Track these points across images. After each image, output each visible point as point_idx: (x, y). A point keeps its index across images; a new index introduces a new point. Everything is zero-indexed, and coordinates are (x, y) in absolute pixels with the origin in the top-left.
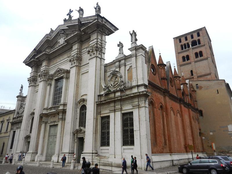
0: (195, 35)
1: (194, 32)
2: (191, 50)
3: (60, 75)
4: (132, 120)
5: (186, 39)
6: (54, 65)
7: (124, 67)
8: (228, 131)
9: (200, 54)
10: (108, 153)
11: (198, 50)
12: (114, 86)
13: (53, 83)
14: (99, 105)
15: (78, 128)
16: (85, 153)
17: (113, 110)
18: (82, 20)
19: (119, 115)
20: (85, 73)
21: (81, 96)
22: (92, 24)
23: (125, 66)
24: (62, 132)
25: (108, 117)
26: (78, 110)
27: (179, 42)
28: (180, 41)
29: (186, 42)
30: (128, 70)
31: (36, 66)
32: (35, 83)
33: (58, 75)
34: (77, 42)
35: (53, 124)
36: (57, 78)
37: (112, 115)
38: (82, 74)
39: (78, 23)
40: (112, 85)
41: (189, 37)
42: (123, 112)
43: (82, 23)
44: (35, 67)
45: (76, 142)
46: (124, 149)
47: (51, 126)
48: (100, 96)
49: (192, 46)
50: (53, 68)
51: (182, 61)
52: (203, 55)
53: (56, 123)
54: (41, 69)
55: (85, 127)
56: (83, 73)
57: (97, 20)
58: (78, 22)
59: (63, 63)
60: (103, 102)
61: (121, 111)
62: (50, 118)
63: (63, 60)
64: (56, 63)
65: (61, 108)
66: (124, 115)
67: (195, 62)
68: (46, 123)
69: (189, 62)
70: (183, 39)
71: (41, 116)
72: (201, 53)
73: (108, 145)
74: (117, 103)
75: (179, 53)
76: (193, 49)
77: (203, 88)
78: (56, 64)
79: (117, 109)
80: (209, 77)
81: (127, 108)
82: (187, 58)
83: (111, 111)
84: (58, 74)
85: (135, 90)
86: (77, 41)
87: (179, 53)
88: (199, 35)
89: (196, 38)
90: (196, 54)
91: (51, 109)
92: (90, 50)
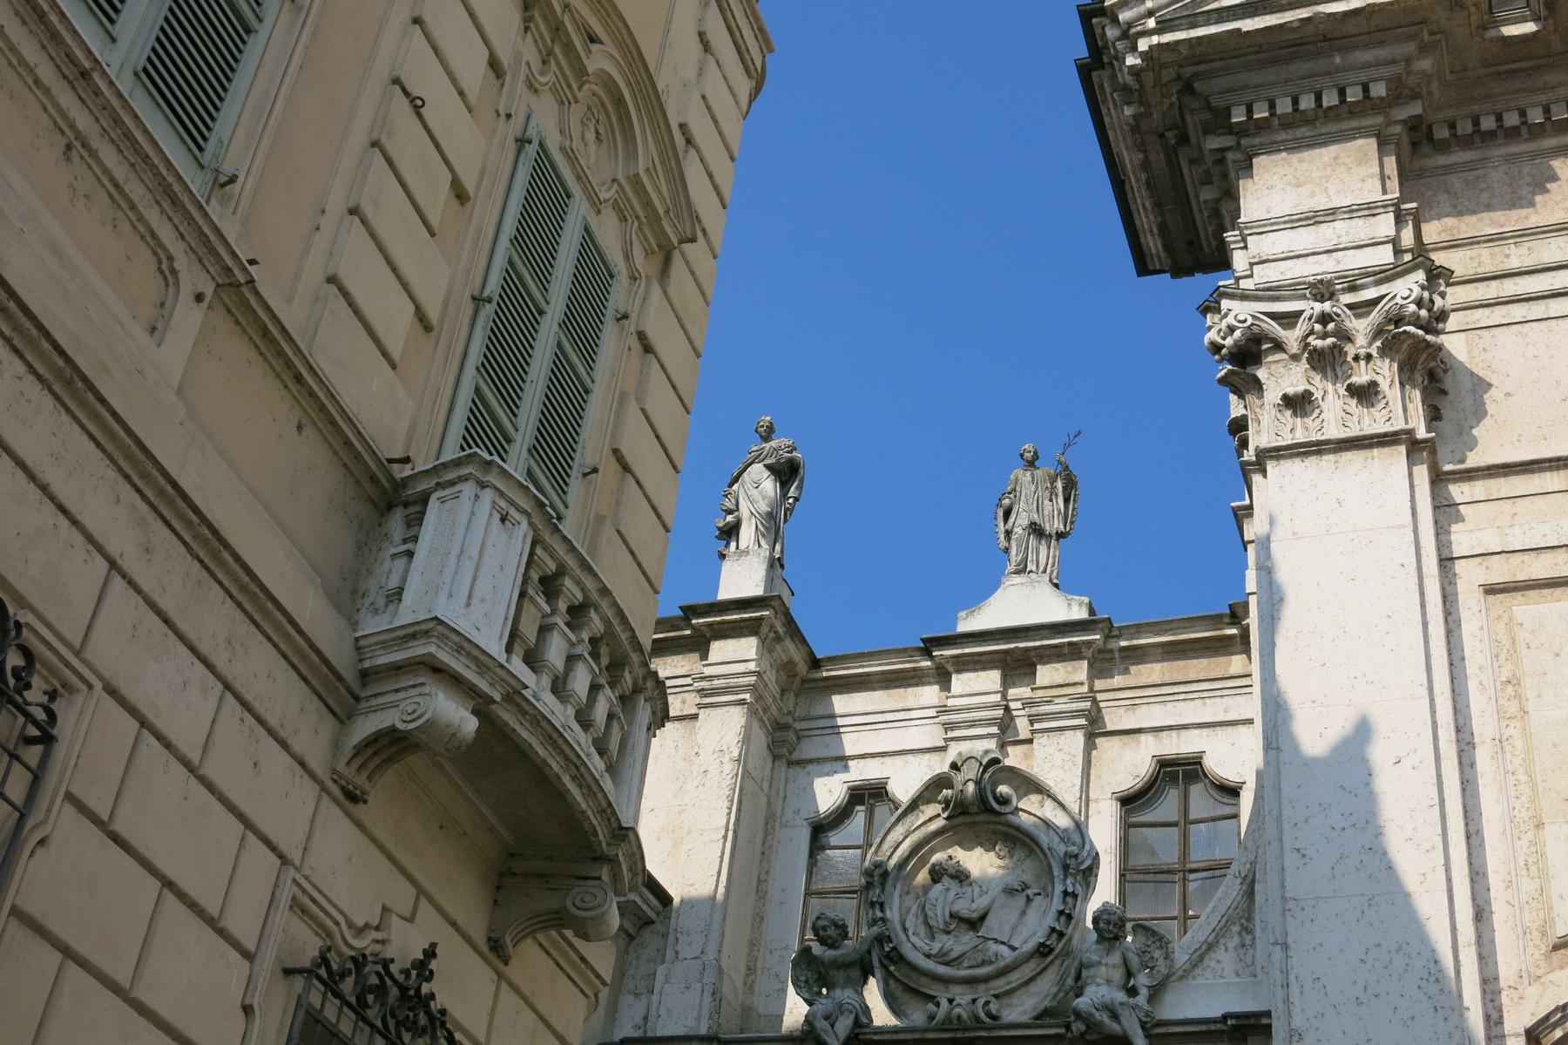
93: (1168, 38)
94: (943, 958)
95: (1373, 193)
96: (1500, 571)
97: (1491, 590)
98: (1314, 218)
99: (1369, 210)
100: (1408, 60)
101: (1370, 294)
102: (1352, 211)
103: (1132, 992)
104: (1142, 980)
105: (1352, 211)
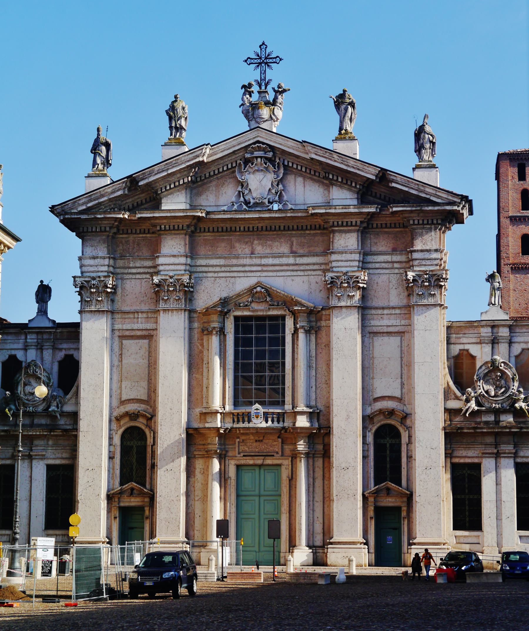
3: (266, 311)
6: (222, 262)
7: (507, 345)
10: (479, 543)
12: (496, 396)
13: (230, 326)
16: (419, 544)
17: (493, 453)
18: (399, 179)
20: (383, 333)
21: (376, 400)
22: (436, 208)
23: (510, 343)
24: (311, 489)
25: (477, 467)
26: (370, 439)
31: (115, 233)
32: (113, 301)
33: (254, 306)
34: (357, 228)
35: (259, 462)
36: (246, 313)
37: (488, 464)
38: (370, 333)
39: (374, 178)
42: (519, 460)
43: (394, 185)
44: (108, 236)
45: (371, 518)
50: (218, 269)
53: (269, 461)
54: (161, 260)
55: (398, 482)
56: (375, 329)
58: (376, 176)
60: (466, 431)
61: (514, 457)
62: (239, 442)
63: (272, 257)
64: (237, 257)
74: (505, 439)
78: (235, 262)
79: (505, 453)
83: (483, 453)
86: (356, 225)
87: (514, 220)
92: (417, 278)
93: (67, 216)
94: (27, 400)
97: (119, 336)
98: (94, 258)
99: (104, 258)
100: (113, 224)
101: (102, 279)
102: (101, 258)
103: (58, 408)
104: (60, 405)
105: (101, 258)
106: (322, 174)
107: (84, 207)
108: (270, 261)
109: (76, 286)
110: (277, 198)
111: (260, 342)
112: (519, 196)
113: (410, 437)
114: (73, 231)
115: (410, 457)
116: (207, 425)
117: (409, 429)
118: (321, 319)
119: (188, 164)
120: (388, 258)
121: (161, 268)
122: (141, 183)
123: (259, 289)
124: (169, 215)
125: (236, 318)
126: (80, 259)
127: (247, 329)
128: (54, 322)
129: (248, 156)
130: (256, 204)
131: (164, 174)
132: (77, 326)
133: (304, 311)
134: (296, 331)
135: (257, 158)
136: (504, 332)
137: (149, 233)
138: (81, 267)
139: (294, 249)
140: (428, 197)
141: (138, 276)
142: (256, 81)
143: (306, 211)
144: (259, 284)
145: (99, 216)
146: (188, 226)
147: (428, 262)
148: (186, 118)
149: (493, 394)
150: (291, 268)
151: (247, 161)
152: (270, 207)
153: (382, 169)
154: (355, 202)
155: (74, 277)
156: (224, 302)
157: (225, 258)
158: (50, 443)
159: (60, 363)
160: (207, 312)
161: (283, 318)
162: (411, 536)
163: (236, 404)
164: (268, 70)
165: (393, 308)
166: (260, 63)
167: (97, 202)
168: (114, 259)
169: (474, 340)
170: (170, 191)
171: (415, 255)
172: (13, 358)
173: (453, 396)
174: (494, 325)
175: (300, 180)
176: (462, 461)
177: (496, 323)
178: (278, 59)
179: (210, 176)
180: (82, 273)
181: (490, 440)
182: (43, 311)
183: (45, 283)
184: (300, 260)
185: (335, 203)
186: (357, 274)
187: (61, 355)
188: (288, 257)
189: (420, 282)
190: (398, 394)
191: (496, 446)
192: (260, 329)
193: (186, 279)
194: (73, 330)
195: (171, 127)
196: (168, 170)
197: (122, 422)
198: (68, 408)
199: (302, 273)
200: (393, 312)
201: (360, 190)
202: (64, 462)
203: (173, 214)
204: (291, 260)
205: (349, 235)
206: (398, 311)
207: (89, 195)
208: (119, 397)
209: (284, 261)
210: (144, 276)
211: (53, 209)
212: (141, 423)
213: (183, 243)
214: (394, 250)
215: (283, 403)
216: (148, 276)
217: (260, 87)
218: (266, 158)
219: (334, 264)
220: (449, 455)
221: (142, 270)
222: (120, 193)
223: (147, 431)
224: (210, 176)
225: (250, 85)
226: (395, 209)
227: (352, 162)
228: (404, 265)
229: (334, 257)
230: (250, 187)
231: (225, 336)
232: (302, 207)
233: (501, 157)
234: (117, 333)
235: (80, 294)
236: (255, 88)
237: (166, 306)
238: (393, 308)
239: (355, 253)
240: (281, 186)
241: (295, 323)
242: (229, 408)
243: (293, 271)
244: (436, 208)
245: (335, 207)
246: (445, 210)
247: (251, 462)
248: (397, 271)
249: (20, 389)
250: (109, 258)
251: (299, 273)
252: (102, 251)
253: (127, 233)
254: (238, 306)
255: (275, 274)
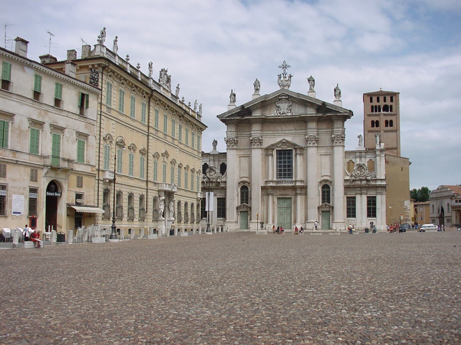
0: (388, 98)
1: (388, 94)
2: (382, 116)
3: (286, 148)
4: (375, 201)
5: (378, 101)
6: (272, 132)
8: (404, 206)
9: (388, 123)
11: (389, 119)
13: (275, 153)
14: (346, 188)
15: (321, 204)
19: (365, 198)
21: (322, 176)
22: (341, 114)
23: (365, 158)
25: (355, 198)
26: (320, 189)
27: (369, 101)
28: (371, 101)
29: (378, 104)
30: (368, 162)
33: (282, 147)
36: (280, 149)
37: (358, 197)
38: (320, 155)
39: (321, 104)
40: (358, 174)
41: (381, 98)
43: (327, 107)
46: (368, 220)
47: (278, 198)
48: (345, 180)
49: (383, 111)
50: (270, 135)
51: (371, 126)
52: (393, 126)
53: (288, 197)
54: (252, 132)
57: (347, 114)
59: (288, 134)
60: (351, 186)
63: (288, 130)
64: (277, 131)
65: (298, 184)
66: (368, 197)
67: (385, 131)
68: (273, 195)
69: (378, 129)
70: (375, 99)
71: (263, 188)
72: (391, 122)
73: (354, 216)
74: (363, 189)
75: (369, 115)
76: (385, 115)
77: (389, 164)
78: (276, 132)
80: (395, 151)
81: (372, 193)
82: (374, 124)
84: (282, 145)
85: (379, 183)
87: (369, 115)
88: (392, 101)
89: (388, 103)
90: (386, 122)
91: (278, 182)
95: (234, 131)
96: (240, 156)
98: (231, 132)
99: (234, 132)
106: (304, 103)
107: (227, 115)
108: (288, 132)
109: (225, 141)
110: (289, 111)
111: (285, 158)
112: (371, 108)
113: (333, 188)
114: (224, 123)
115: (333, 195)
116: (268, 185)
117: (333, 186)
118: (304, 151)
119: (261, 101)
120: (326, 130)
121: (252, 135)
122: (245, 108)
123: (284, 141)
124: (254, 117)
125: (277, 150)
126: (226, 132)
127: (280, 154)
128: (218, 152)
129: (280, 98)
130: (283, 113)
131: (253, 104)
132: (226, 153)
133: (299, 148)
134: (296, 155)
135: (283, 98)
136: (363, 154)
137: (248, 123)
138: (227, 134)
139: (295, 128)
140: (338, 110)
141: (245, 137)
142: (282, 73)
143: (299, 115)
144: (284, 139)
145: (232, 118)
146: (261, 121)
147: (339, 132)
148: (260, 86)
149: (360, 174)
150: (294, 134)
151: (280, 99)
152: (287, 115)
153: (323, 102)
154: (315, 113)
155: (225, 138)
156: (273, 145)
157: (273, 131)
158: (218, 191)
159: (220, 165)
160: (267, 149)
161: (292, 150)
162: (333, 219)
163: (277, 178)
164: (286, 70)
165: (328, 147)
166: (283, 68)
167: (231, 114)
168: (237, 132)
169: (354, 157)
170: (255, 110)
171: (335, 129)
172: (205, 164)
173: (347, 175)
174: (360, 152)
175: (297, 105)
176: (350, 196)
177: (361, 151)
178: (289, 66)
179: (268, 105)
180: (227, 136)
181: (359, 189)
182: (215, 148)
183: (215, 140)
184: (297, 131)
185: (308, 113)
186: (316, 136)
187: (221, 163)
188: (293, 130)
189: (336, 138)
190: (329, 175)
191: (361, 191)
192: (285, 154)
193: (260, 138)
194: (225, 155)
195: (255, 89)
196: (254, 103)
197: (241, 184)
198: (223, 180)
199: (298, 136)
200: (327, 148)
201: (316, 108)
202: (222, 197)
203: (256, 117)
204: (294, 132)
205: (313, 123)
206: (329, 148)
207: (229, 112)
208: (239, 176)
209: (292, 132)
210: (247, 137)
211: (217, 116)
212: (246, 184)
213: (259, 126)
214: (328, 128)
215: (292, 178)
216: (248, 137)
217: (284, 75)
218: (286, 98)
219: (308, 133)
220: (345, 194)
221: (246, 135)
222: (239, 111)
223: (248, 187)
224: (268, 105)
225: (280, 75)
226: (328, 115)
227: (314, 100)
228: (331, 133)
229: (308, 130)
230: (281, 108)
231: (273, 156)
232: (298, 114)
233: (364, 94)
234: (239, 156)
235: (227, 143)
236: (282, 76)
237: (254, 147)
238: (328, 147)
239: (315, 129)
240: (291, 108)
241: (296, 152)
242: (275, 179)
243: (295, 135)
244: (341, 114)
245: (308, 114)
246: (344, 115)
247: (282, 197)
248: (328, 135)
249: (208, 174)
250: (236, 132)
251: (297, 136)
252: (233, 129)
253: (241, 123)
254: (277, 147)
255: (289, 136)
